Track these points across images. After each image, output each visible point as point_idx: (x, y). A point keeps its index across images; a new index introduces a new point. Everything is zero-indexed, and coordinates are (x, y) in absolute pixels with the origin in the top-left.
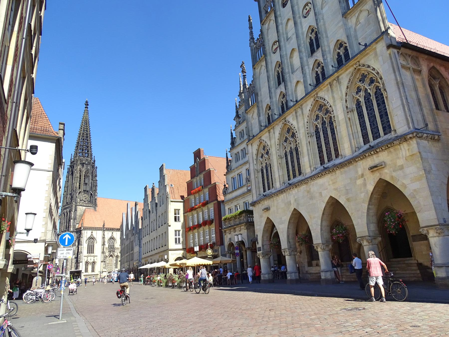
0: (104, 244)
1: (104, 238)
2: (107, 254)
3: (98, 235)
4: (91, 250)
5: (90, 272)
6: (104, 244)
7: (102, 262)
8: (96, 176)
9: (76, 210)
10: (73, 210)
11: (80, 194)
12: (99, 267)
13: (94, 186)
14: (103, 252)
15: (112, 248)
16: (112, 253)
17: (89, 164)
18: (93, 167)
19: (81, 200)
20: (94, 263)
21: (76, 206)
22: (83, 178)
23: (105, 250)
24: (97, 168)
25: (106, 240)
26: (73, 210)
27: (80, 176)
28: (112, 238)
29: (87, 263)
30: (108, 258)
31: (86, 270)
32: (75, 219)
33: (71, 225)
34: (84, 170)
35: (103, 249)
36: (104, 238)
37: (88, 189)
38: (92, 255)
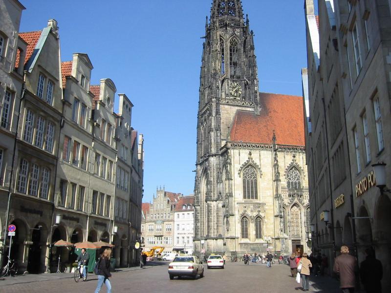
0: (277, 180)
1: (276, 166)
2: (287, 201)
3: (264, 159)
4: (251, 190)
5: (252, 238)
6: (277, 180)
7: (276, 216)
8: (252, 48)
9: (218, 113)
10: (214, 114)
11: (225, 83)
12: (271, 227)
13: (252, 65)
14: (277, 197)
15: (294, 189)
16: (296, 200)
17: (238, 25)
18: (245, 30)
19: (227, 95)
20: (258, 220)
21: (218, 104)
22: (227, 52)
23: (280, 192)
24: (252, 32)
25: (282, 172)
26: (214, 114)
27: (223, 50)
28: (294, 167)
29: (244, 219)
30: (288, 210)
31: (245, 234)
32: (218, 129)
33: (211, 143)
34: (227, 37)
35: (277, 190)
36: (276, 166)
37: (238, 73)
38: (255, 201)
